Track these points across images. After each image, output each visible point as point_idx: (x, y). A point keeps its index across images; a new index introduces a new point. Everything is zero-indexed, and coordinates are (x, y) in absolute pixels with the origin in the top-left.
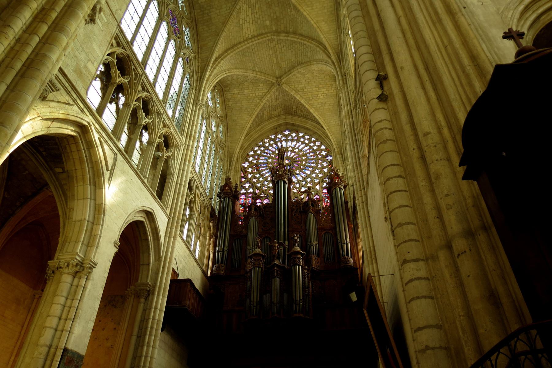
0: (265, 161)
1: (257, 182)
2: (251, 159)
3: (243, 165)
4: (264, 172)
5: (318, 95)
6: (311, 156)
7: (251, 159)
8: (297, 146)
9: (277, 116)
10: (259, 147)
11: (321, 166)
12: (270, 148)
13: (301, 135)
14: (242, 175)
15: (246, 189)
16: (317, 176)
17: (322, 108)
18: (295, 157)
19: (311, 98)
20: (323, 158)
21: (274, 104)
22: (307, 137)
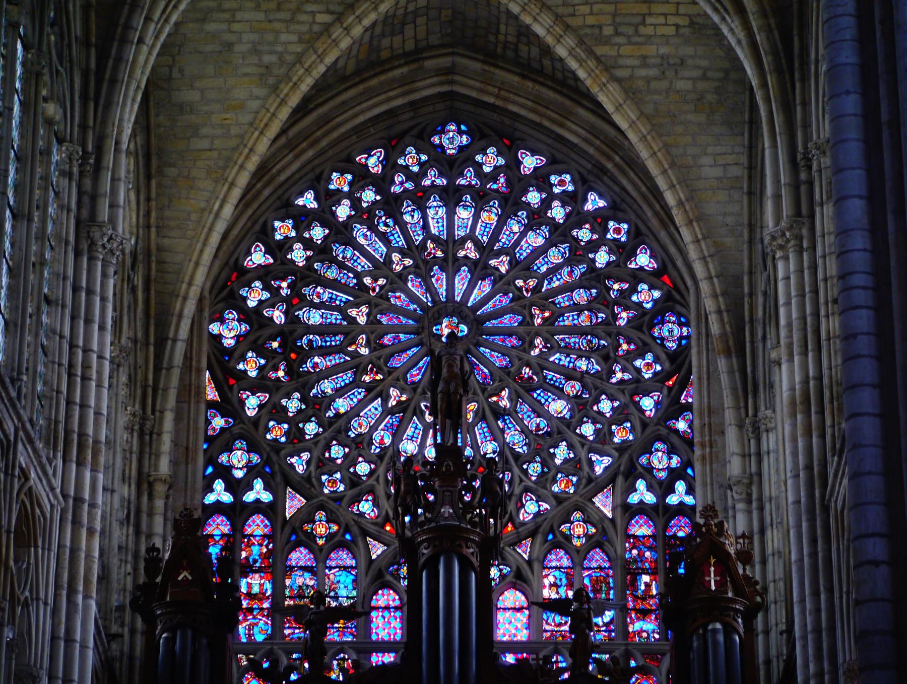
0: (334, 317)
1: (290, 448)
2: (255, 296)
3: (215, 328)
4: (327, 386)
5: (649, 20)
6: (578, 309)
7: (255, 296)
8: (504, 239)
9: (405, 54)
10: (303, 219)
11: (627, 376)
12: (360, 233)
13: (529, 162)
14: (212, 394)
15: (233, 486)
16: (603, 438)
17: (664, 84)
18: (489, 307)
19: (608, 31)
20: (639, 328)
21: (401, 12)
22: (562, 183)
